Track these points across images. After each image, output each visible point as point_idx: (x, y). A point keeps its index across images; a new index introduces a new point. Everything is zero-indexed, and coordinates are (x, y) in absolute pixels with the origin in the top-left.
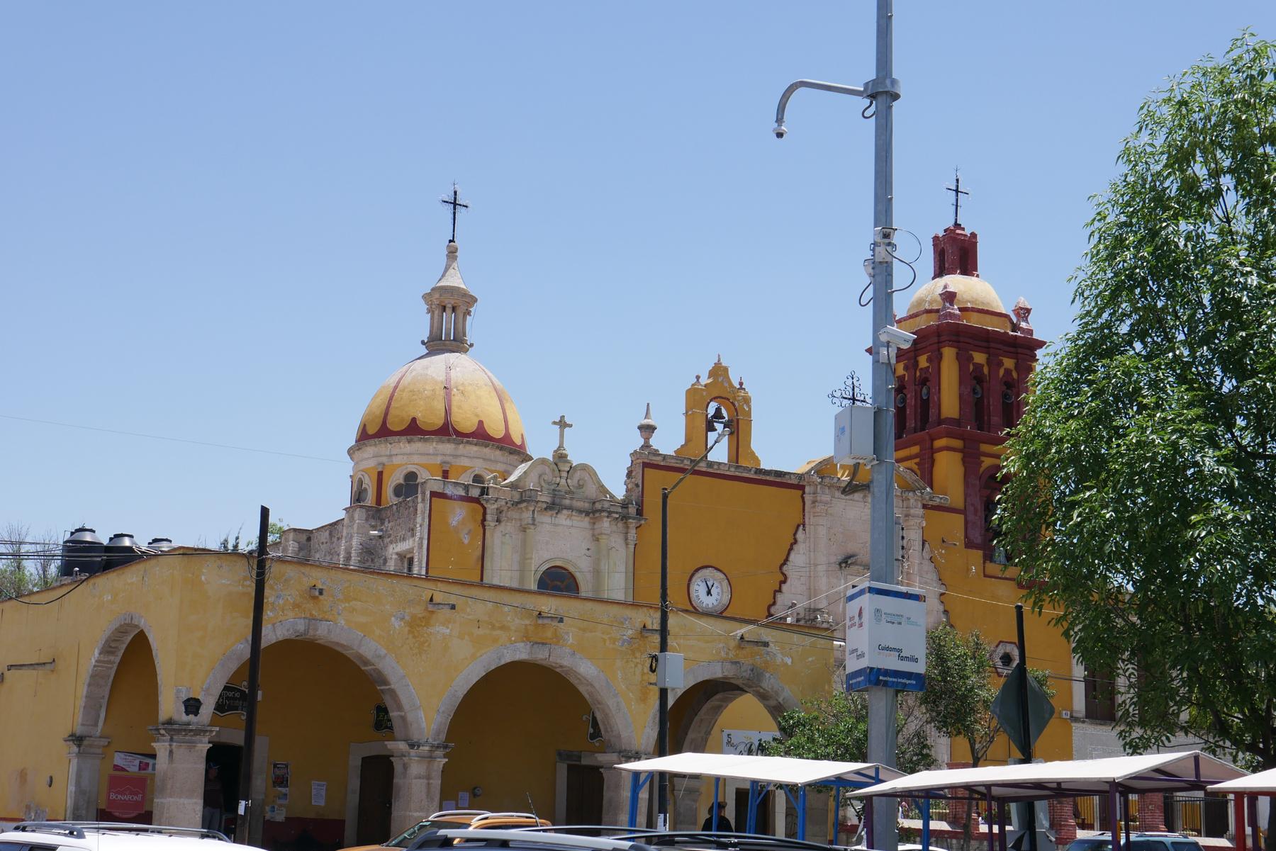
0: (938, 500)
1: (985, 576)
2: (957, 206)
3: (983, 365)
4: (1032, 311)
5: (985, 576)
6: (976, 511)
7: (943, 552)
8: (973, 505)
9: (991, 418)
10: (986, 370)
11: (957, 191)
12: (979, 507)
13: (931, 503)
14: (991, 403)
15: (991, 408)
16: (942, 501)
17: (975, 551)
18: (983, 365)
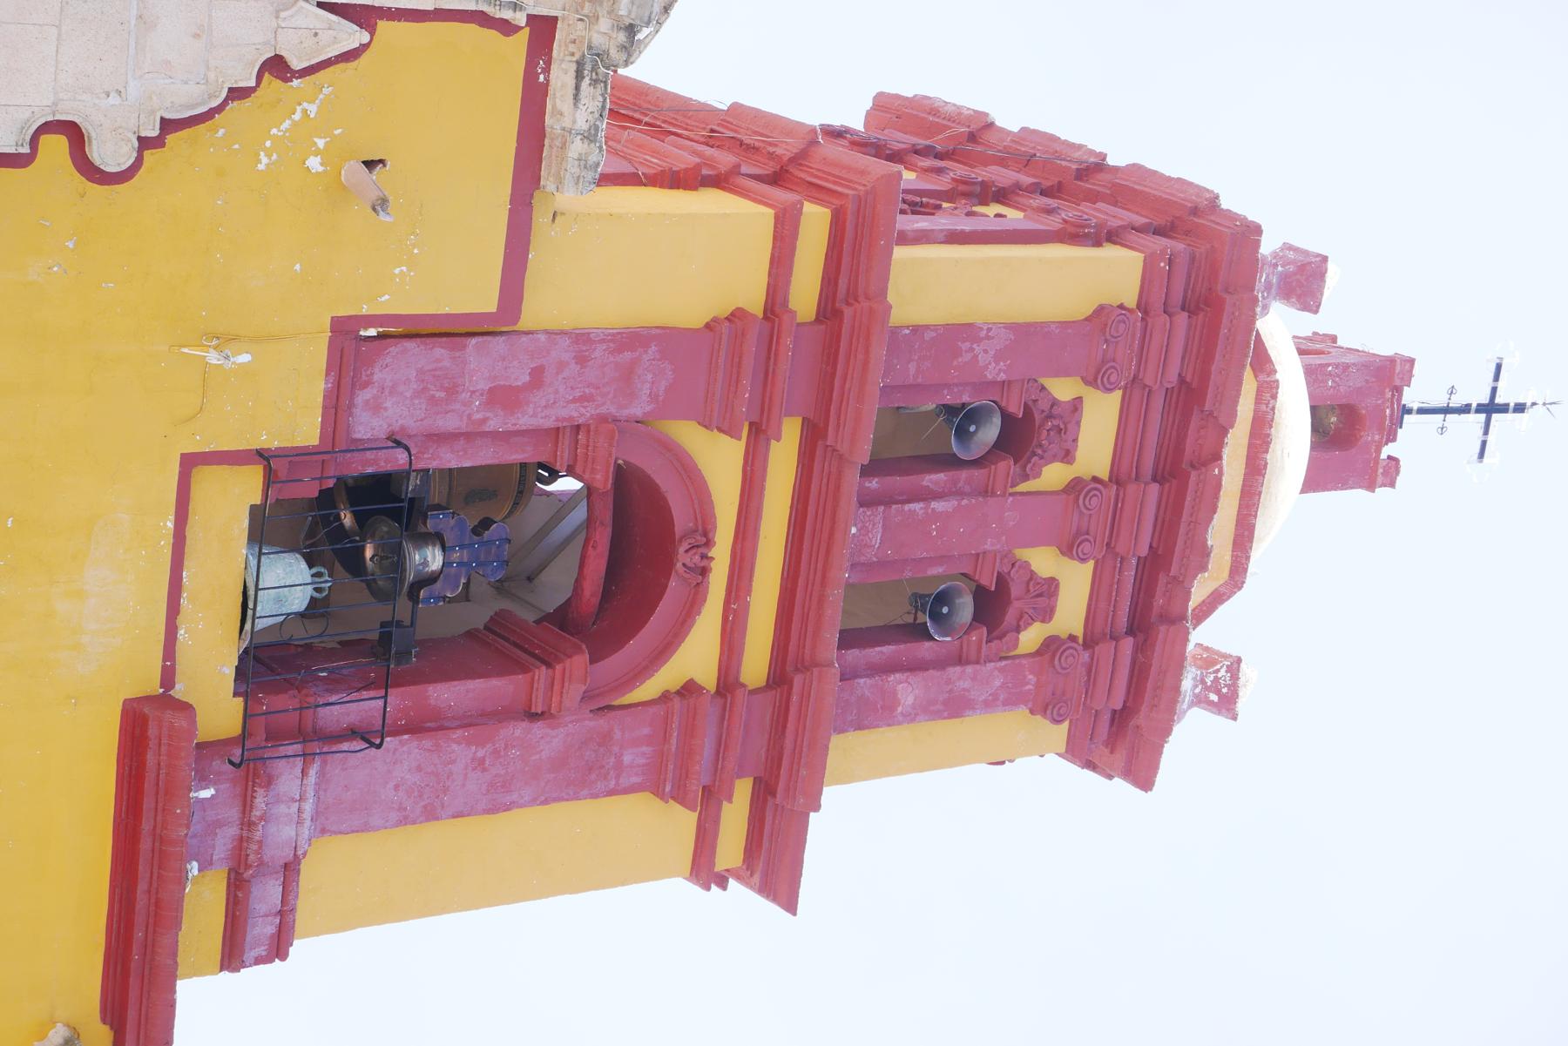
0: (582, 124)
1: (190, 462)
2: (1446, 410)
3: (1068, 456)
4: (1220, 721)
5: (190, 462)
6: (504, 397)
7: (314, 163)
8: (537, 376)
9: (881, 508)
10: (1054, 475)
11: (1490, 408)
12: (525, 420)
13: (561, 76)
14: (938, 506)
15: (917, 507)
16: (577, 147)
17: (316, 388)
18: (1068, 456)
